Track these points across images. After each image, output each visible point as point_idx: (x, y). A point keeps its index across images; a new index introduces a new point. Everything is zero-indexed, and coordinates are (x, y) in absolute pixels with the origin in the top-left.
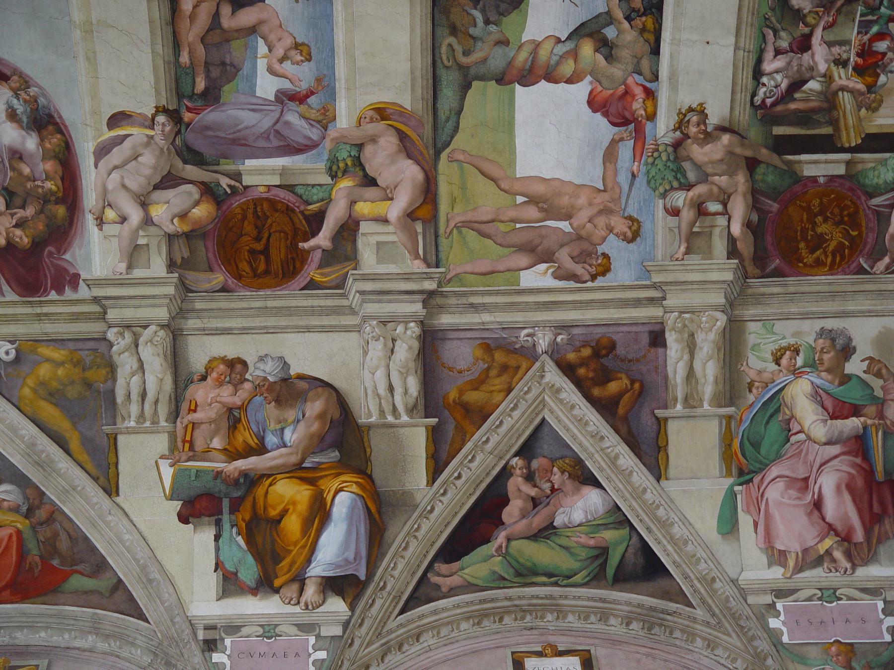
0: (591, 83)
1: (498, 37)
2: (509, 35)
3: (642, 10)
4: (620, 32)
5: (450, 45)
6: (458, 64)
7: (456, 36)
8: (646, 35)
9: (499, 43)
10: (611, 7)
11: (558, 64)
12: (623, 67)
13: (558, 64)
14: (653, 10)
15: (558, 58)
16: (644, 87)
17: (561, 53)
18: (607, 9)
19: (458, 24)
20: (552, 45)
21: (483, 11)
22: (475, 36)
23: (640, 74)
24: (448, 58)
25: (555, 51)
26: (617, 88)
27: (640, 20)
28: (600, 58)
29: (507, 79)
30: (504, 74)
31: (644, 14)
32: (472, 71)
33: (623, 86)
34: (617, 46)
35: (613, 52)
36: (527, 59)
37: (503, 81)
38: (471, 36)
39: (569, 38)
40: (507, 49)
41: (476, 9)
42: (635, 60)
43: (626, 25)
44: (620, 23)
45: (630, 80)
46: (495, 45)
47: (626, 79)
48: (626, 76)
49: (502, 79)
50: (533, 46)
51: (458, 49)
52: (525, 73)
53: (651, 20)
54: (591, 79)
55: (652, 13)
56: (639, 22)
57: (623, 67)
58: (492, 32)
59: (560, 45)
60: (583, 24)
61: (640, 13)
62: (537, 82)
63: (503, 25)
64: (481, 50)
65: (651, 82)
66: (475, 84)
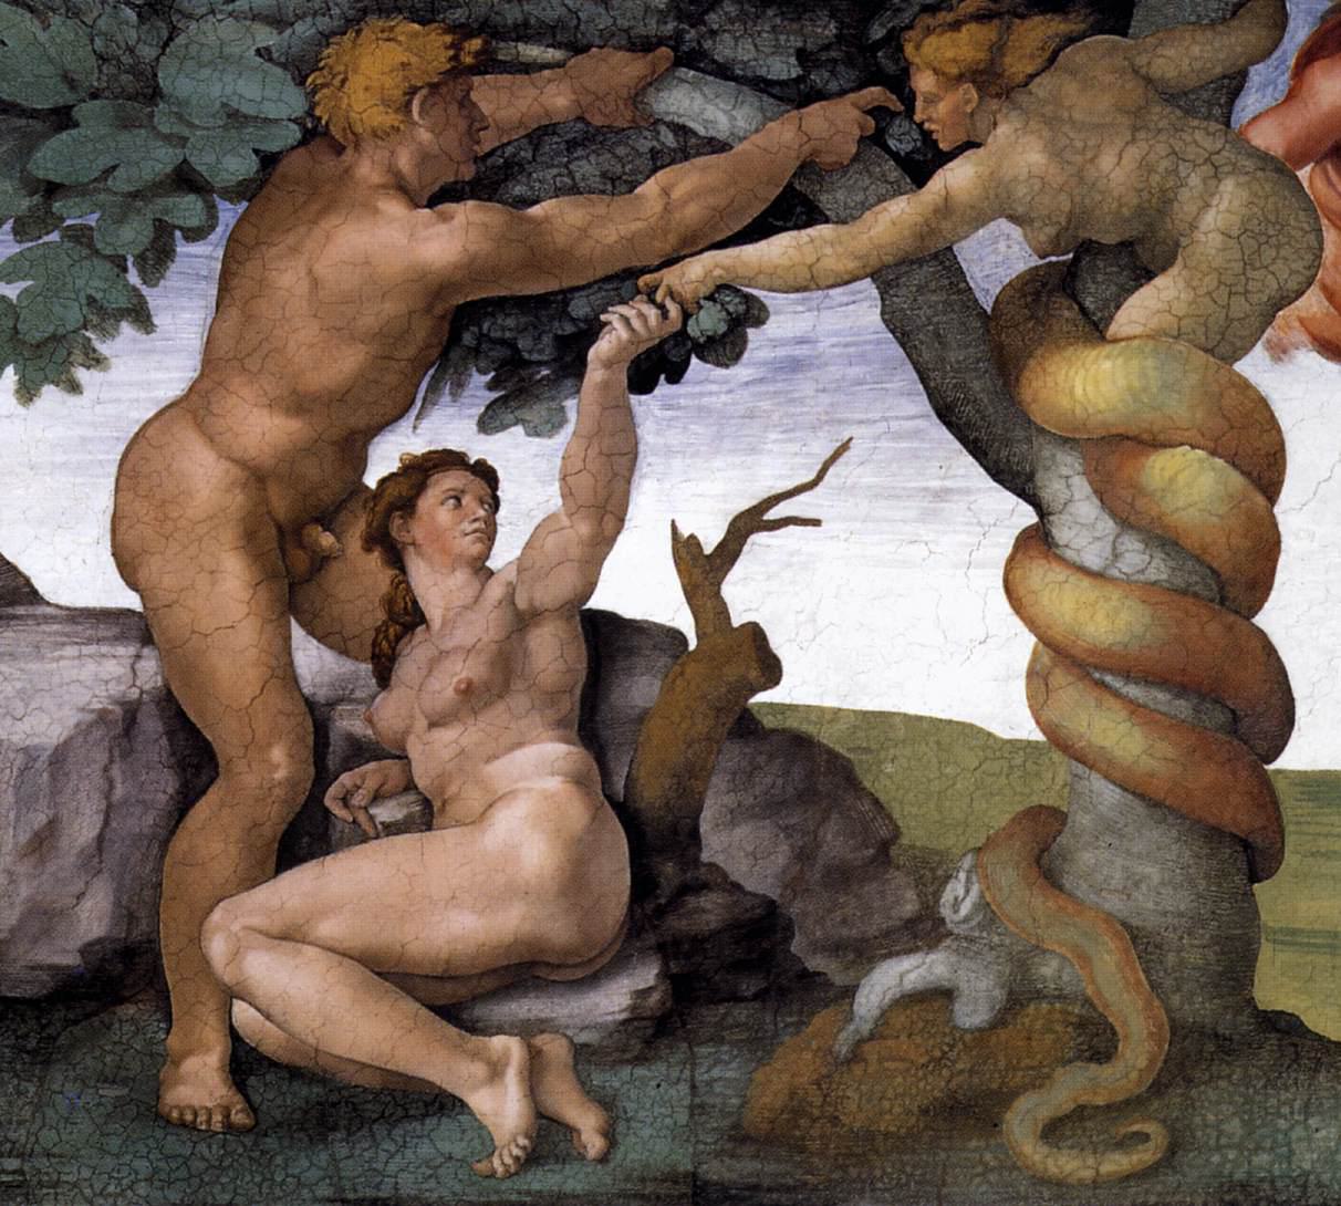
0: (1279, 352)
1: (1009, 876)
2: (1000, 815)
3: (874, 94)
4: (997, 204)
5: (1053, 1132)
6: (1158, 1088)
7: (1005, 1098)
8: (1017, 65)
9: (1046, 867)
10: (851, 265)
11: (1163, 539)
12: (1195, 180)
13: (1163, 539)
14: (877, 32)
15: (1132, 547)
16: (1310, 55)
17: (1108, 525)
18: (867, 287)
19: (935, 1086)
20: (1058, 573)
21: (865, 953)
22: (999, 994)
23: (1234, 83)
24: (1123, 1144)
25: (1093, 559)
26: (1310, 207)
27: (931, 100)
28: (1142, 309)
29: (1238, 815)
30: (1214, 835)
31: (900, 83)
32: (1200, 1008)
33: (1303, 174)
34: (1078, 217)
35: (1110, 239)
36: (1134, 707)
37: (1258, 840)
38: (999, 1022)
39: (1017, 479)
40: (1082, 820)
41: (849, 992)
42: (1160, 114)
43: (958, 177)
44: (946, 208)
45: (1269, 138)
46: (1060, 888)
47: (1264, 158)
48: (1249, 164)
49: (1246, 845)
50: (1059, 677)
51: (1071, 1086)
52: (1221, 717)
53: (932, 41)
54: (1259, 350)
55: (894, 40)
56: (942, 108)
57: (1195, 180)
58: (983, 905)
59: (1062, 533)
60: (946, 414)
61: (895, 104)
62: (1270, 651)
63: (949, 841)
64: (1085, 959)
65: (1280, 22)
66: (1274, 988)
